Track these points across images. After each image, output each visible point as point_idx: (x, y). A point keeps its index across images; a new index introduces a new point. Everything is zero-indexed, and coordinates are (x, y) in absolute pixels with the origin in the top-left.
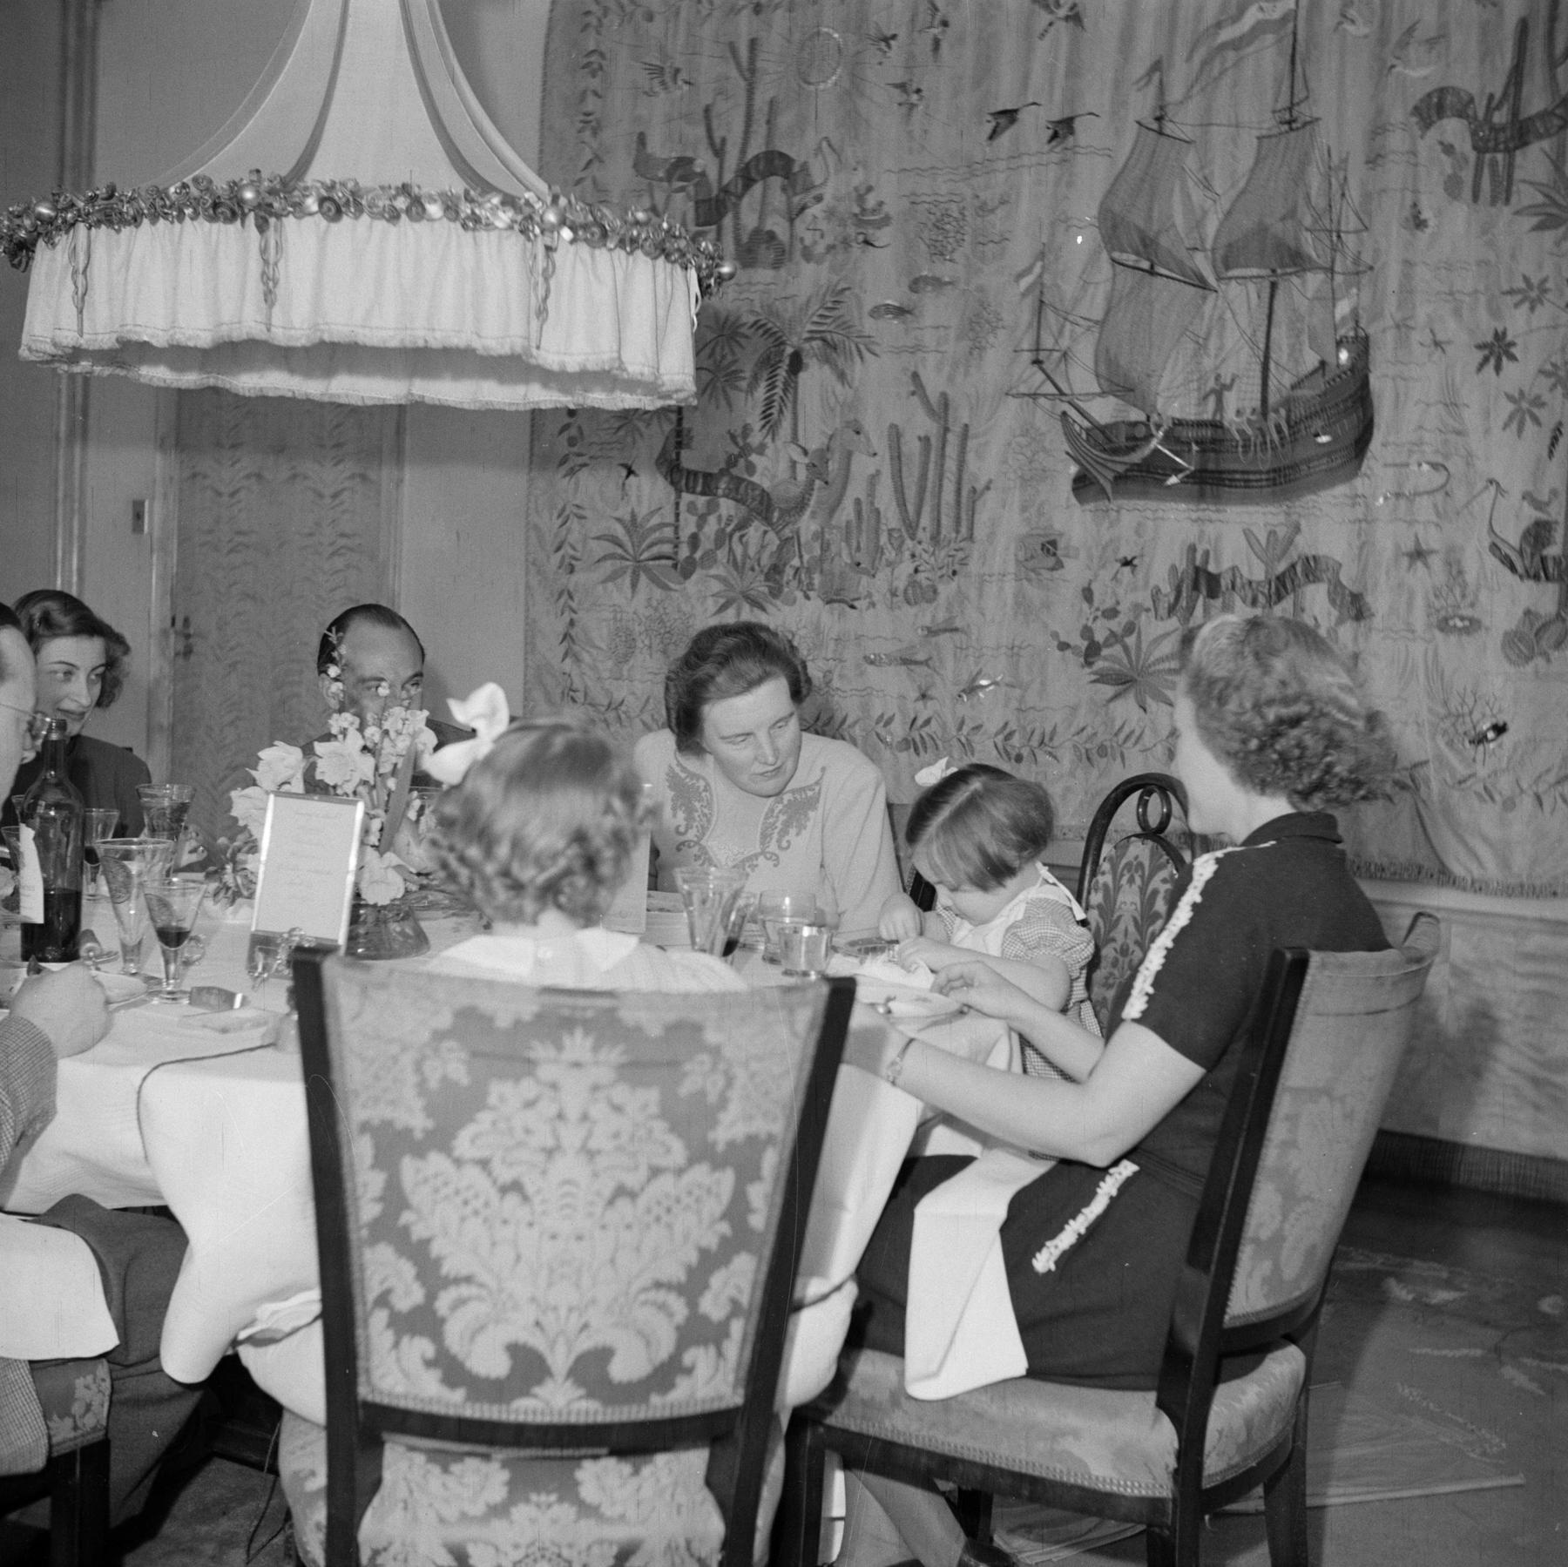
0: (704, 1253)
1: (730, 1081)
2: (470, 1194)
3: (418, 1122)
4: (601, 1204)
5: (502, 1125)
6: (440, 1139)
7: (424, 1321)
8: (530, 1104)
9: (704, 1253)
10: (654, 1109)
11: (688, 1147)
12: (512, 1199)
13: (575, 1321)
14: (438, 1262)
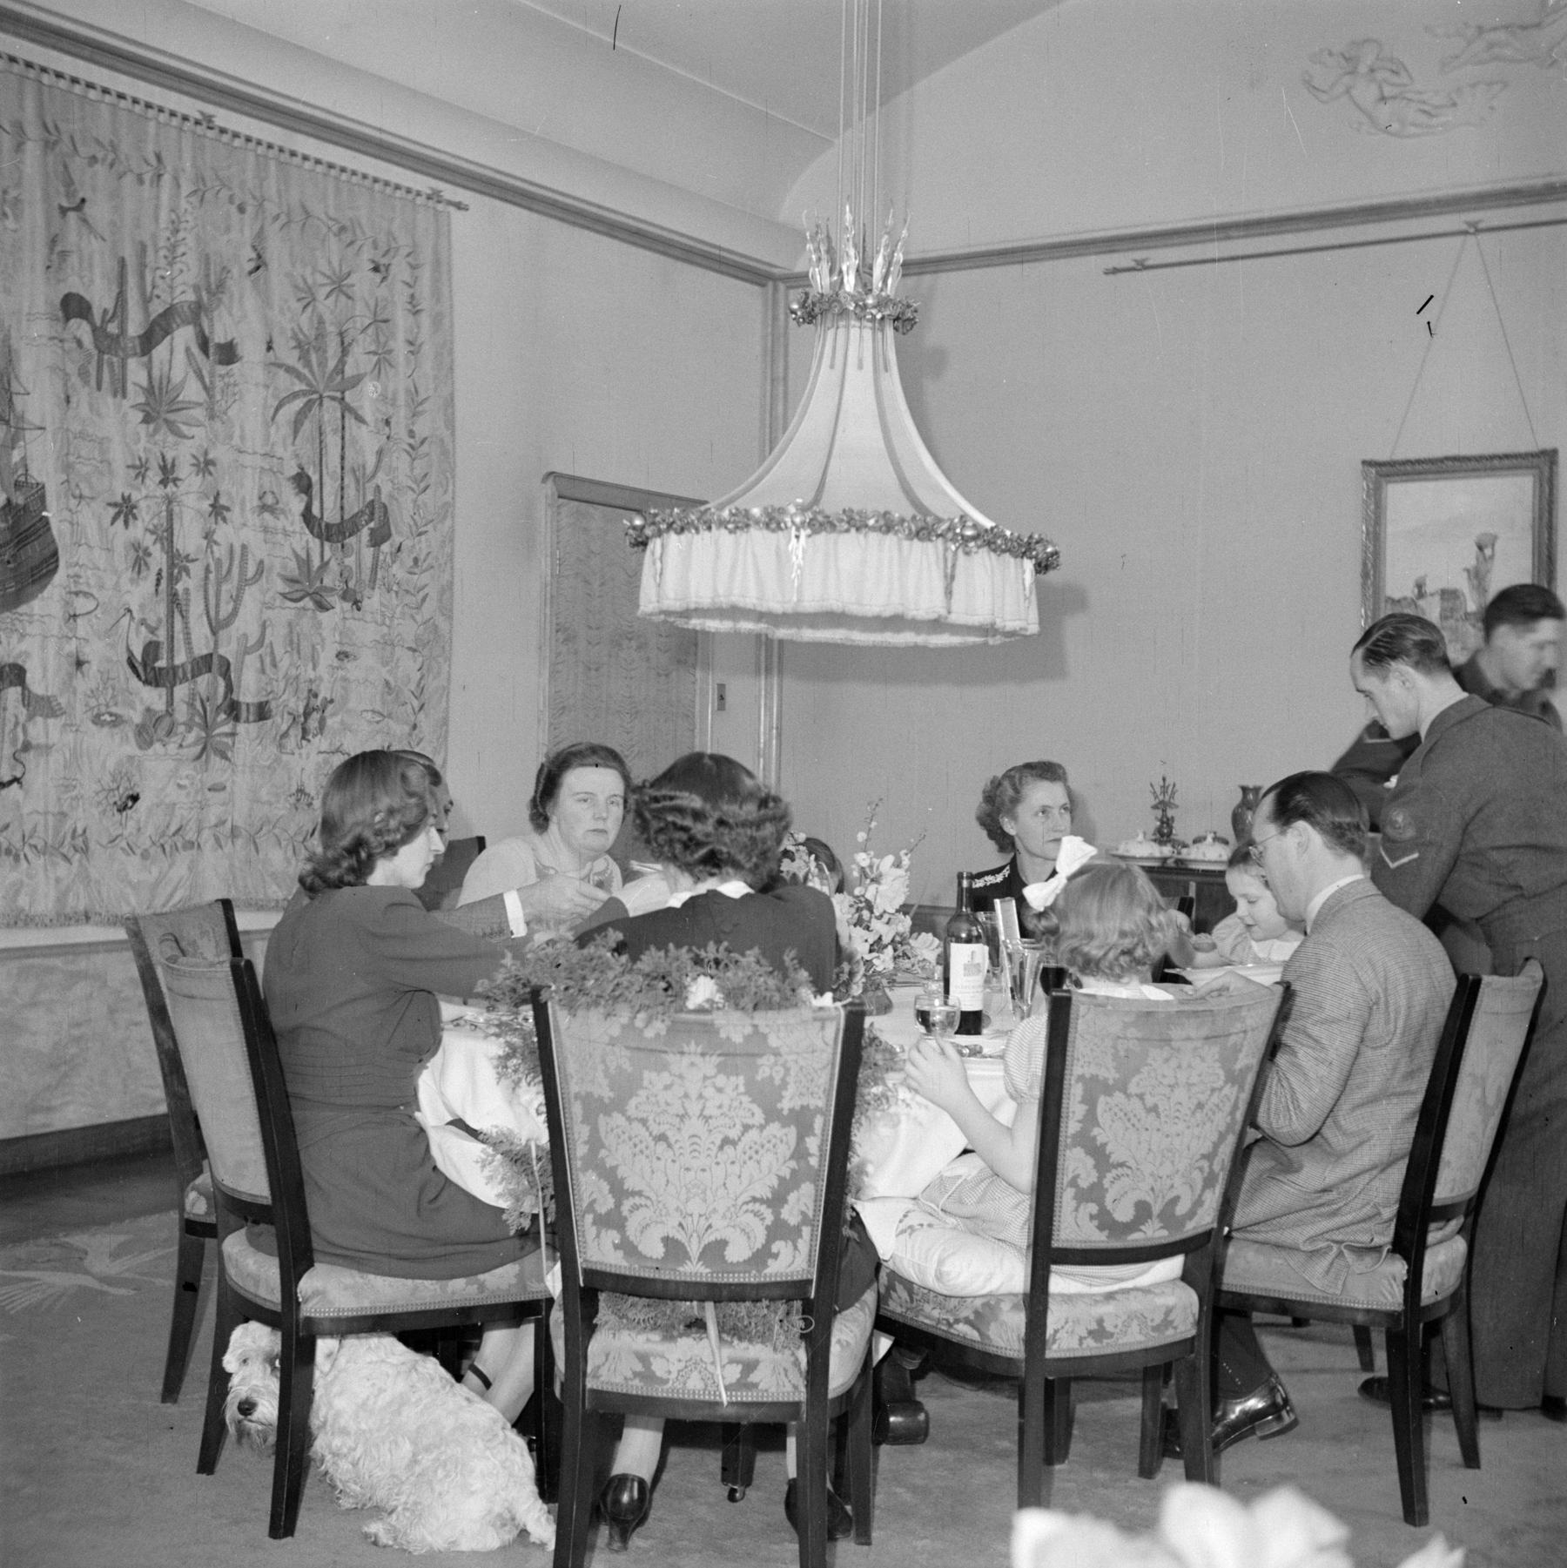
0: (781, 1179)
1: (787, 1070)
2: (637, 1140)
3: (607, 1094)
4: (715, 1149)
5: (653, 1099)
6: (619, 1105)
7: (613, 1221)
8: (667, 1088)
9: (781, 1179)
10: (742, 1089)
11: (765, 1112)
12: (662, 1146)
13: (704, 1223)
14: (622, 1182)
